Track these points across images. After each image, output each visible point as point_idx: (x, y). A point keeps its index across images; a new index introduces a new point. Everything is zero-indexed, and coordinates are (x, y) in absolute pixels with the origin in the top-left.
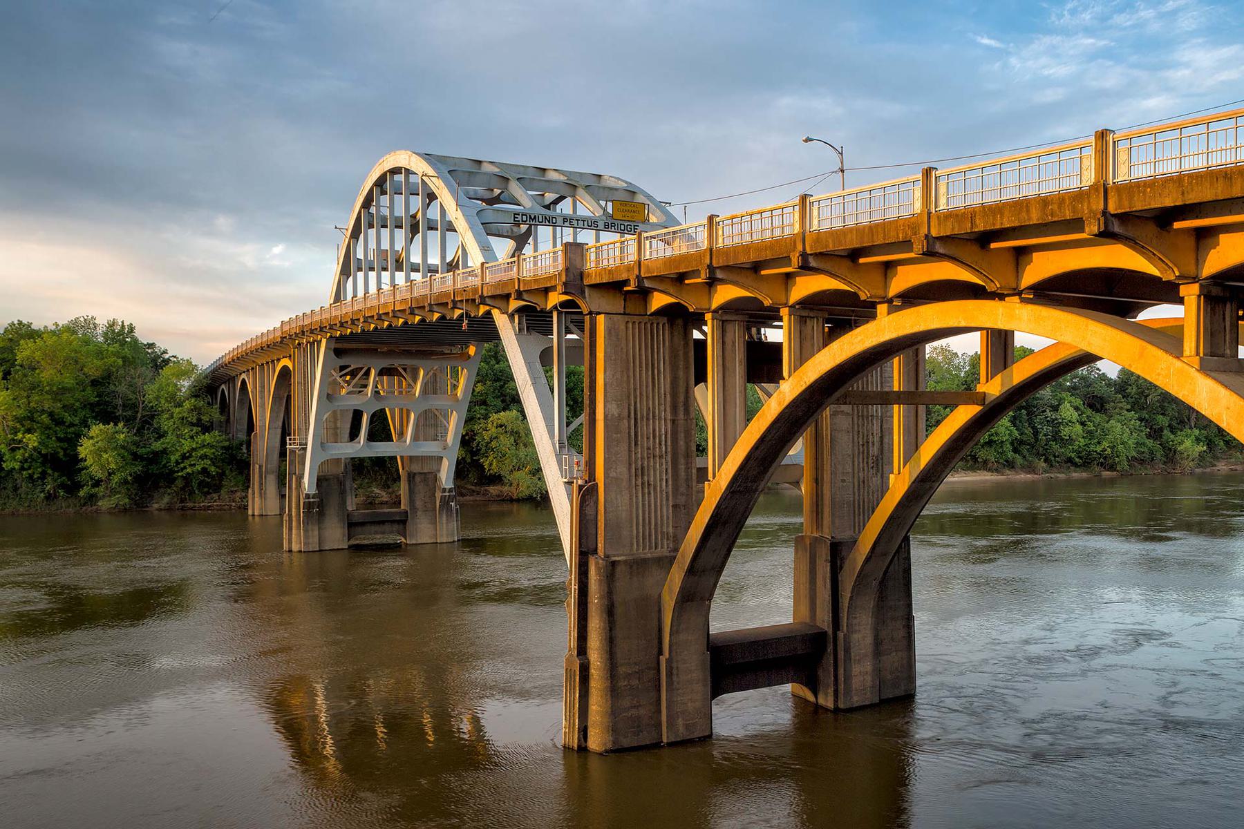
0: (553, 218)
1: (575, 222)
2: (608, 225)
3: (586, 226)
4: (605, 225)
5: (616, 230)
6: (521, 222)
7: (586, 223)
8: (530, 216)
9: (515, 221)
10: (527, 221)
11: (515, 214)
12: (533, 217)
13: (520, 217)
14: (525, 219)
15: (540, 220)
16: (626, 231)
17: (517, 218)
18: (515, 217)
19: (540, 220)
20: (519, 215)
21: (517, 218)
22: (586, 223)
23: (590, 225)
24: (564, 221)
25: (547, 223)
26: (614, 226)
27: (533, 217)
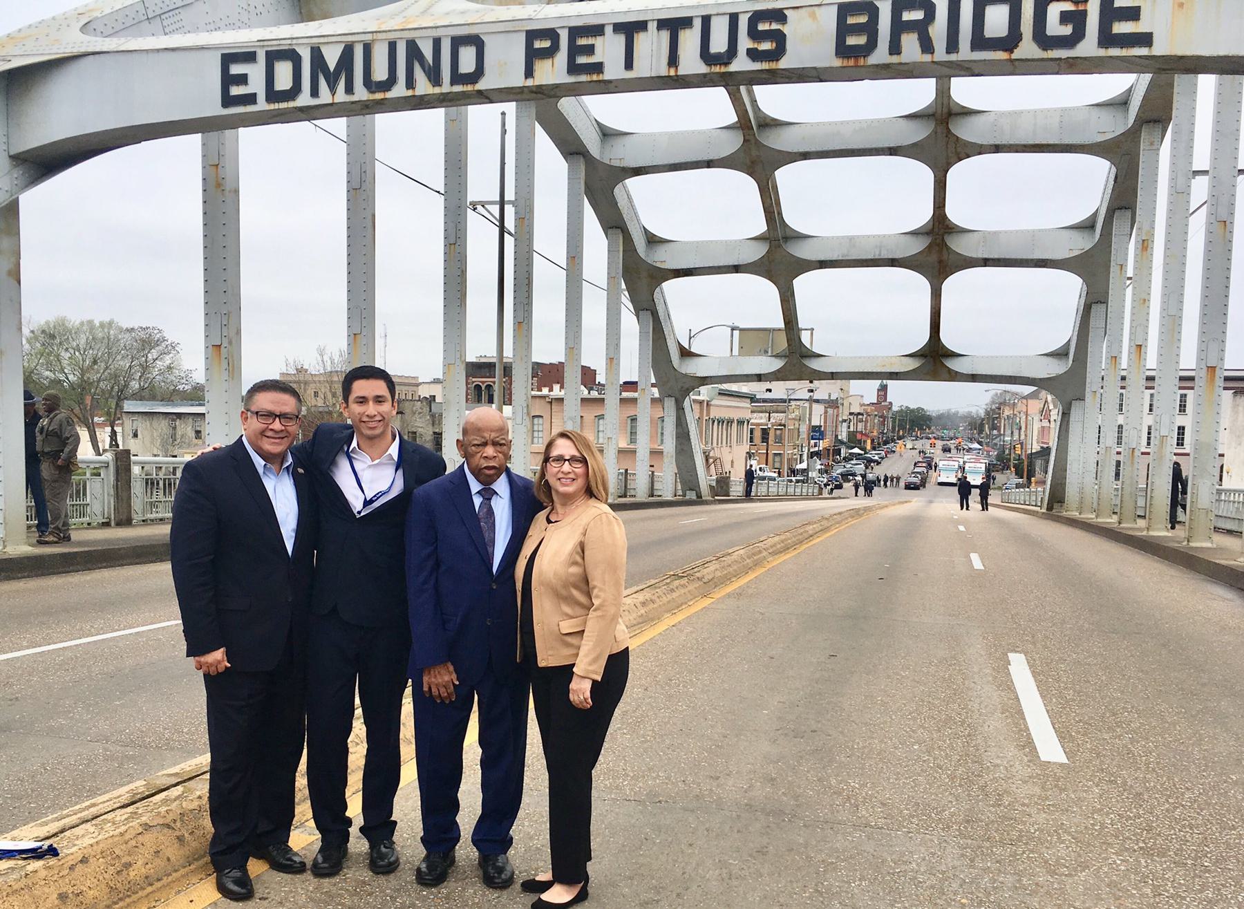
0: (457, 42)
1: (609, 50)
2: (870, 29)
3: (691, 63)
4: (843, 30)
5: (940, 54)
6: (262, 105)
7: (690, 41)
8: (317, 55)
9: (228, 100)
10: (296, 90)
11: (228, 59)
12: (332, 57)
13: (255, 73)
14: (284, 76)
15: (380, 73)
16: (1028, 48)
17: (242, 79)
18: (228, 80)
19: (380, 72)
20: (250, 57)
21: (242, 79)
22: (690, 41)
23: (719, 44)
24: (532, 56)
25: (423, 86)
26: (921, 29)
27: (332, 57)
